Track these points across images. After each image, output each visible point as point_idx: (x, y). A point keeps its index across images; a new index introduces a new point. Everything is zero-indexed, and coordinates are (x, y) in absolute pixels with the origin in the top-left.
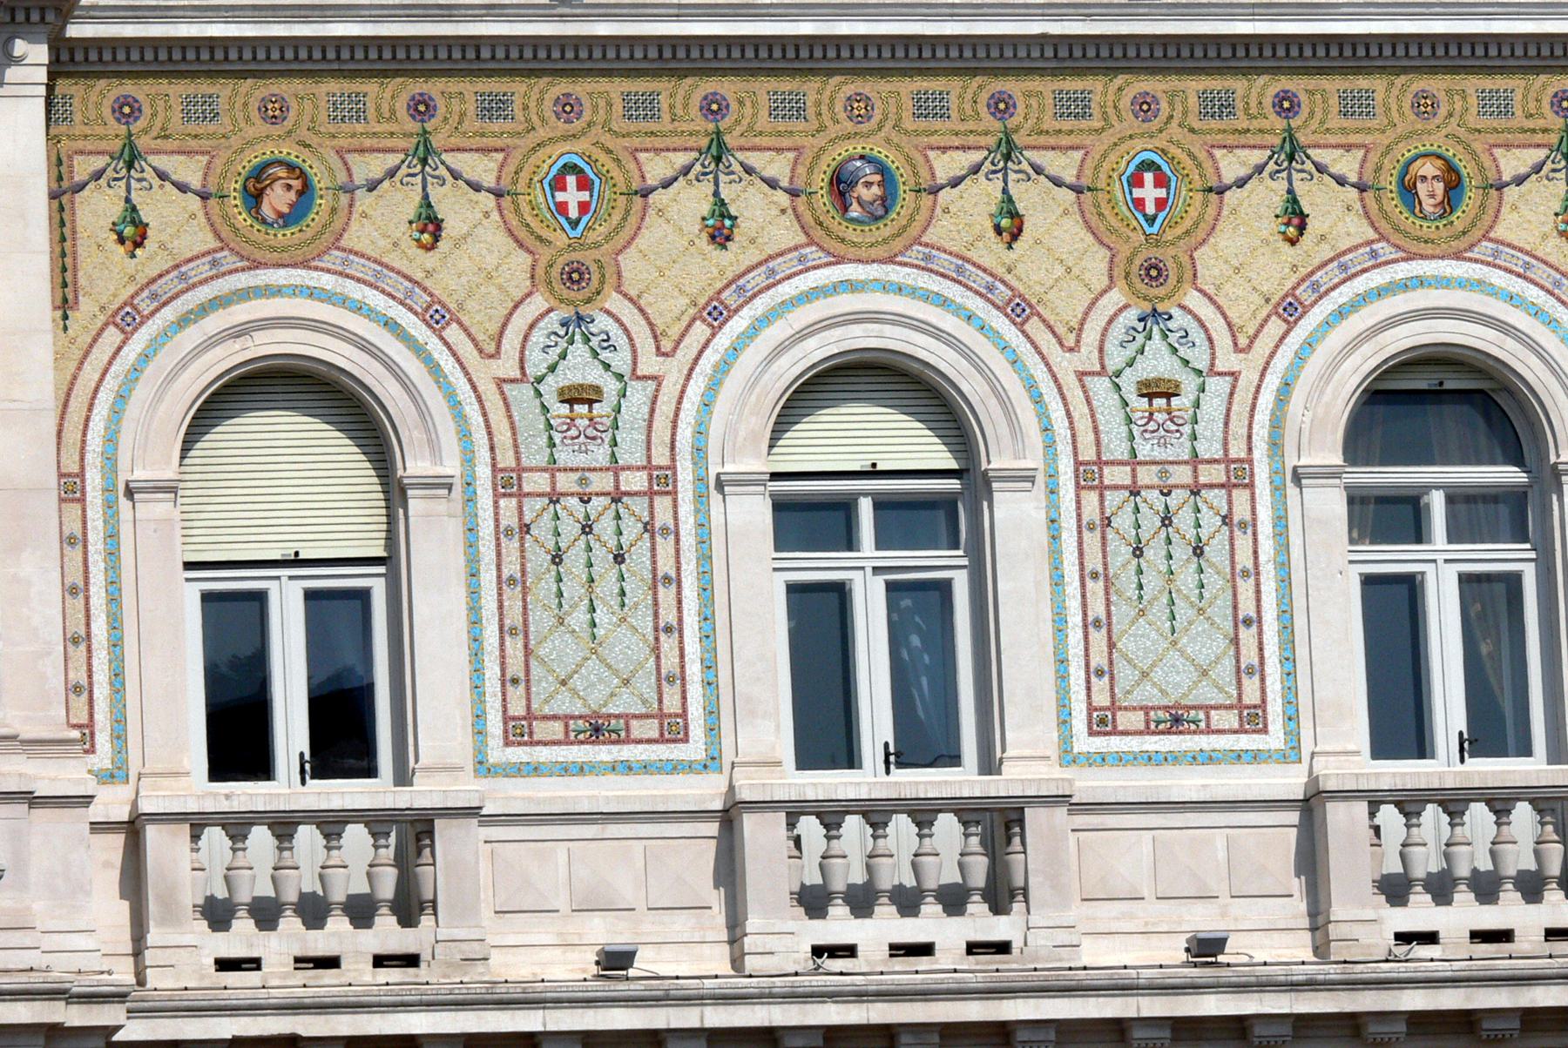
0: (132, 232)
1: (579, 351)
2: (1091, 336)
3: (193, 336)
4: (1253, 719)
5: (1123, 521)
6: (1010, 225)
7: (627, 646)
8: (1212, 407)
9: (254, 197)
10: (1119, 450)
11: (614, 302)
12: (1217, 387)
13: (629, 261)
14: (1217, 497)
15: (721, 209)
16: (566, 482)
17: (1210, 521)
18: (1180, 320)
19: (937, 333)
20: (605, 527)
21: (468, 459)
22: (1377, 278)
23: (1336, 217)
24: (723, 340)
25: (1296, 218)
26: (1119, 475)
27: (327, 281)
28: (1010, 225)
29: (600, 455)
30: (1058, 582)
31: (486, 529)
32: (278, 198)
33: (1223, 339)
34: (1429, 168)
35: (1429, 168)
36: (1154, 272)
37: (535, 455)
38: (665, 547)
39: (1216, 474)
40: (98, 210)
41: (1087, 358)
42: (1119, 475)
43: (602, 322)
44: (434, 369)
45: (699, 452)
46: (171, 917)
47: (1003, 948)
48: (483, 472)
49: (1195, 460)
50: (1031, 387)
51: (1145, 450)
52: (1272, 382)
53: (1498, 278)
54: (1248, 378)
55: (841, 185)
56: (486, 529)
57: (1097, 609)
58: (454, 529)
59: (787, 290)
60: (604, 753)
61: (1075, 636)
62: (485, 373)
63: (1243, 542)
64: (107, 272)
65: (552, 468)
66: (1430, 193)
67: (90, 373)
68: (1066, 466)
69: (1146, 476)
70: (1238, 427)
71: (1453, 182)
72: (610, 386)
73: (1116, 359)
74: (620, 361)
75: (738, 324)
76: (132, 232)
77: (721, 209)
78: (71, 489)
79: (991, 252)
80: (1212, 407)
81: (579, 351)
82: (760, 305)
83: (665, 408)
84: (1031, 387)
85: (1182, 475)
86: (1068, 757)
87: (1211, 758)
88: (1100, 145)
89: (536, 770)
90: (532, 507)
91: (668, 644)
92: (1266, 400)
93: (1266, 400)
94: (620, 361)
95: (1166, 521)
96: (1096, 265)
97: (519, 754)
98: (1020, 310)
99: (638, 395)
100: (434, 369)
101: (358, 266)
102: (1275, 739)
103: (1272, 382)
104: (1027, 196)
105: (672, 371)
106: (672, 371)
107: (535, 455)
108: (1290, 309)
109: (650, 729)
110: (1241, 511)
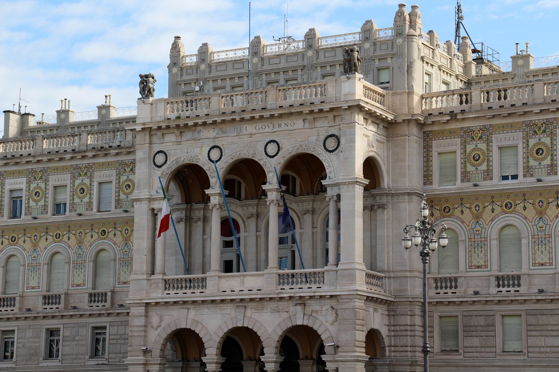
1: (477, 225)
2: (533, 221)
4: (551, 264)
5: (537, 242)
6: (525, 208)
9: (444, 210)
10: (536, 234)
11: (481, 220)
12: (548, 226)
14: (548, 239)
15: (493, 209)
18: (544, 218)
19: (514, 221)
23: (498, 209)
26: (537, 237)
28: (525, 208)
29: (479, 237)
31: (467, 245)
32: (447, 210)
33: (549, 221)
39: (548, 236)
41: (533, 223)
42: (537, 237)
43: (480, 222)
46: (431, 288)
47: (518, 291)
51: (539, 234)
52: (555, 225)
54: (551, 225)
56: (467, 245)
59: (500, 217)
63: (551, 244)
68: (530, 236)
69: (539, 237)
70: (550, 231)
75: (494, 222)
77: (493, 209)
79: (522, 211)
80: (547, 228)
81: (477, 225)
82: (497, 219)
83: (486, 231)
85: (544, 236)
92: (554, 227)
93: (554, 227)
94: (482, 226)
95: (542, 241)
99: (484, 230)
102: (554, 267)
103: (555, 225)
104: (527, 205)
105: (487, 227)
106: (487, 227)
110: (550, 240)
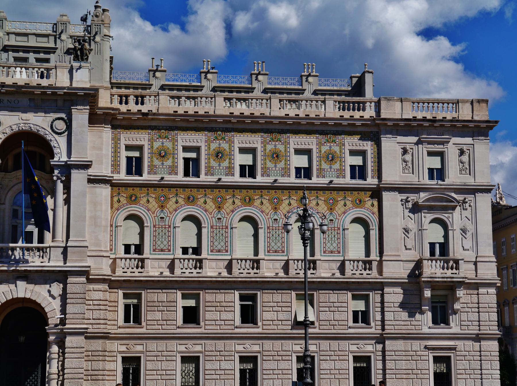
0: (119, 201)
1: (162, 214)
2: (213, 213)
3: (124, 211)
6: (205, 202)
7: (165, 243)
8: (224, 221)
11: (166, 209)
13: (168, 205)
14: (224, 230)
16: (160, 226)
17: (224, 232)
20: (164, 231)
21: (151, 224)
22: (242, 208)
24: (176, 213)
25: (234, 203)
27: (138, 206)
28: (205, 202)
30: (208, 237)
32: (133, 198)
33: (226, 214)
34: (247, 198)
35: (247, 198)
36: (219, 207)
37: (157, 224)
38: (170, 233)
40: (116, 199)
41: (212, 216)
44: (148, 215)
45: (173, 224)
48: (152, 225)
49: (222, 226)
50: (207, 218)
52: (231, 218)
53: (254, 209)
55: (189, 198)
57: (212, 240)
58: (149, 231)
60: (163, 253)
61: (210, 243)
62: (153, 216)
63: (227, 234)
64: (116, 205)
65: (159, 225)
66: (247, 200)
67: (114, 215)
71: (250, 199)
72: (165, 217)
73: (215, 216)
74: (166, 215)
75: (178, 211)
76: (119, 201)
78: (111, 226)
79: (203, 205)
80: (224, 221)
81: (162, 214)
84: (207, 218)
86: (208, 254)
87: (222, 255)
88: (215, 195)
89: (156, 254)
90: (157, 229)
91: (169, 242)
96: (214, 207)
97: (154, 253)
98: (206, 211)
100: (148, 215)
101: (141, 205)
103: (231, 218)
105: (171, 216)
106: (171, 216)
107: (157, 224)
108: (233, 211)
109: (167, 250)
